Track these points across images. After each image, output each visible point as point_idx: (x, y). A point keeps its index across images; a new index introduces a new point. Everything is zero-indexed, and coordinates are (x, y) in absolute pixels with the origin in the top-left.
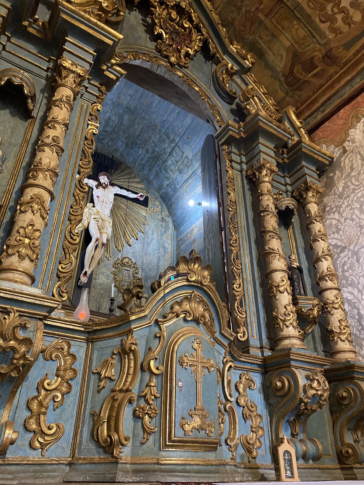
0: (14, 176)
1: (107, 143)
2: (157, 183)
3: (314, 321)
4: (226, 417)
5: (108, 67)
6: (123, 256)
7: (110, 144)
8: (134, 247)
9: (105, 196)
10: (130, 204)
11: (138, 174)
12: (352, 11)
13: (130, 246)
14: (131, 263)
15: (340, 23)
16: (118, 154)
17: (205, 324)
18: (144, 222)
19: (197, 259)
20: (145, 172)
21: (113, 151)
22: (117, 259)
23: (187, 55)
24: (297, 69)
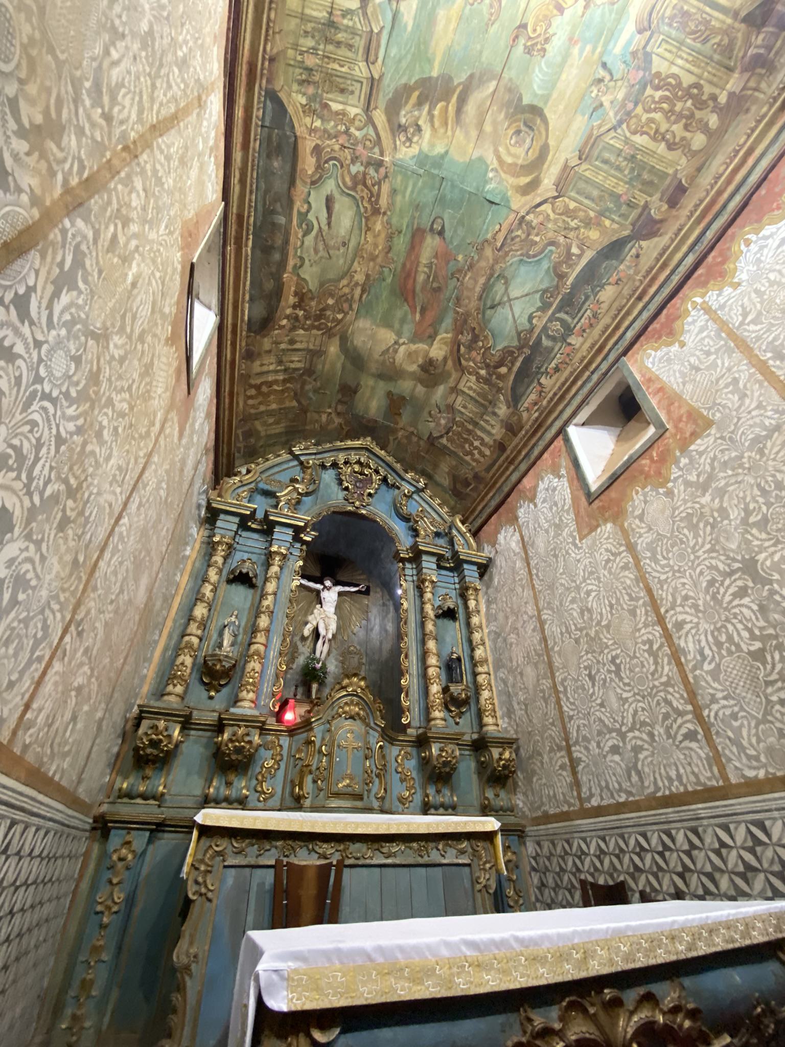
0: (245, 632)
3: (466, 702)
9: (330, 596)
12: (483, 449)
15: (477, 456)
19: (355, 675)
23: (370, 495)
24: (458, 486)
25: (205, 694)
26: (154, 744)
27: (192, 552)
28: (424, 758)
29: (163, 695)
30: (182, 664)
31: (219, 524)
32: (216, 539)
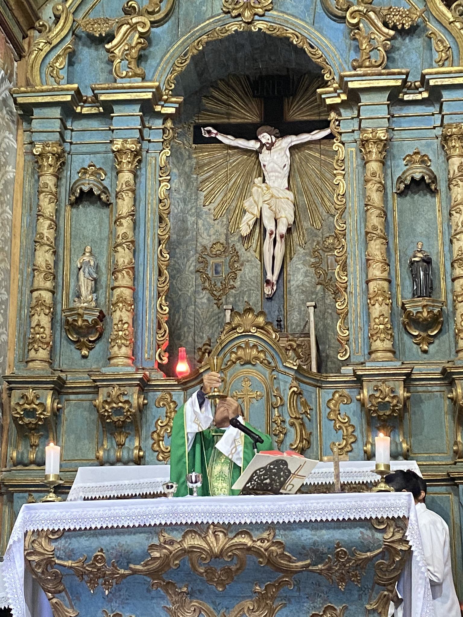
4: (292, 430)
5: (163, 106)
7: (273, 58)
10: (324, 144)
16: (294, 64)
17: (261, 362)
25: (76, 354)
26: (30, 413)
27: (15, 171)
28: (359, 400)
29: (27, 362)
30: (38, 325)
31: (36, 125)
32: (37, 151)
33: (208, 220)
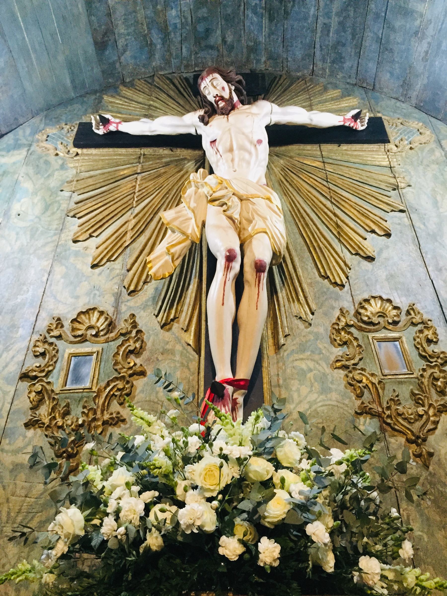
1: (224, 41)
2: (392, 74)
6: (359, 298)
7: (229, 39)
8: (387, 259)
11: (331, 83)
13: (370, 259)
14: (395, 312)
16: (263, 59)
18: (393, 181)
20: (348, 64)
21: (248, 58)
22: (337, 313)
33: (79, 266)
